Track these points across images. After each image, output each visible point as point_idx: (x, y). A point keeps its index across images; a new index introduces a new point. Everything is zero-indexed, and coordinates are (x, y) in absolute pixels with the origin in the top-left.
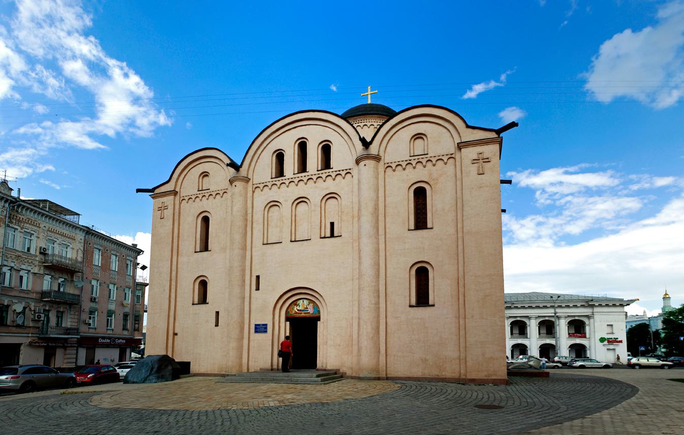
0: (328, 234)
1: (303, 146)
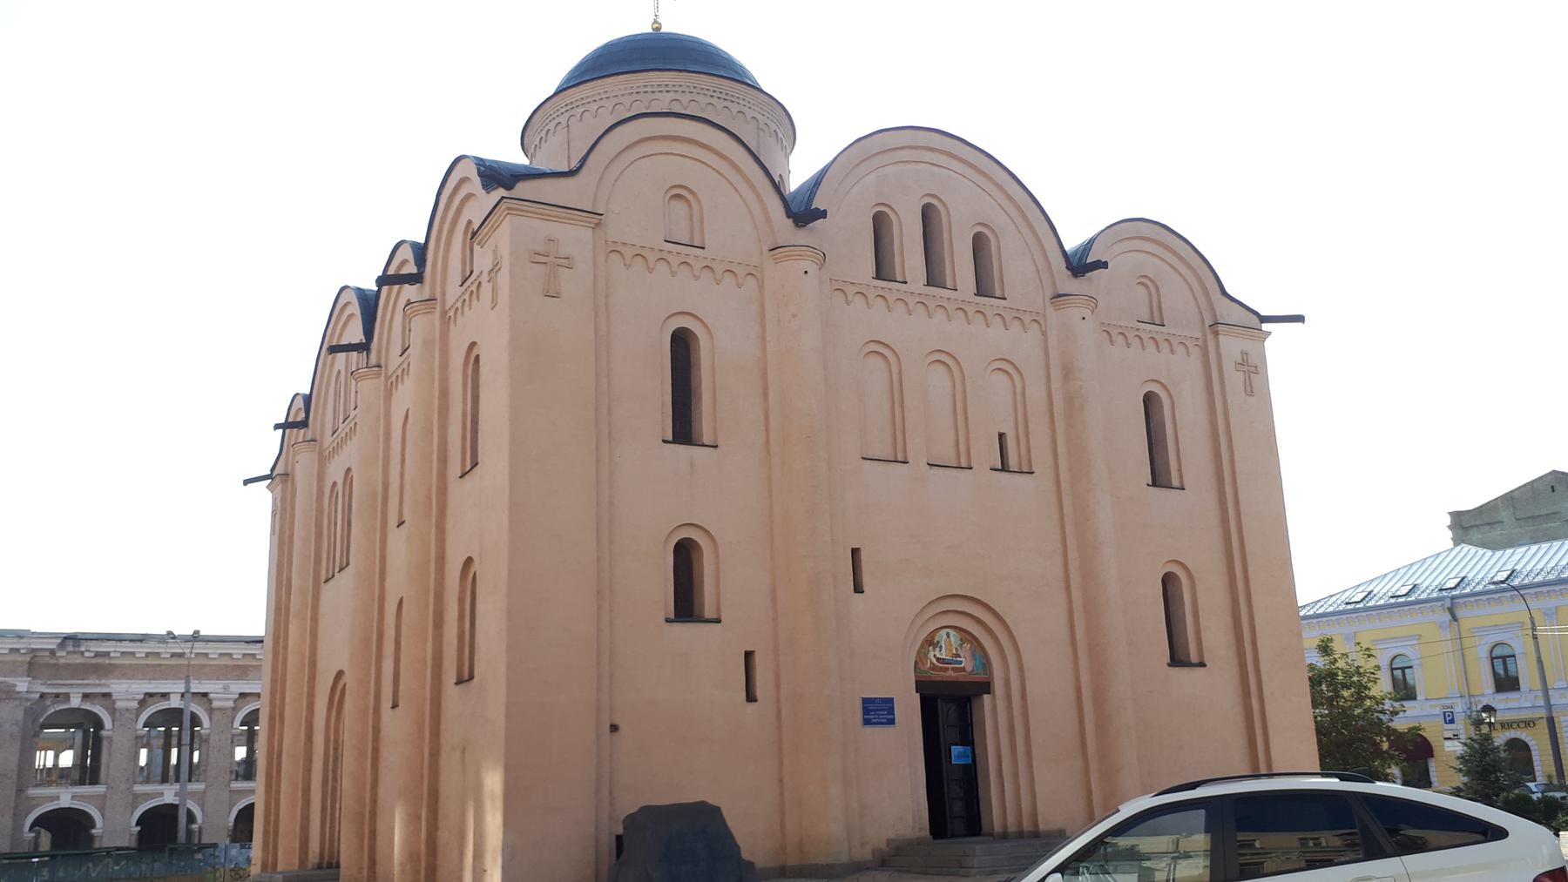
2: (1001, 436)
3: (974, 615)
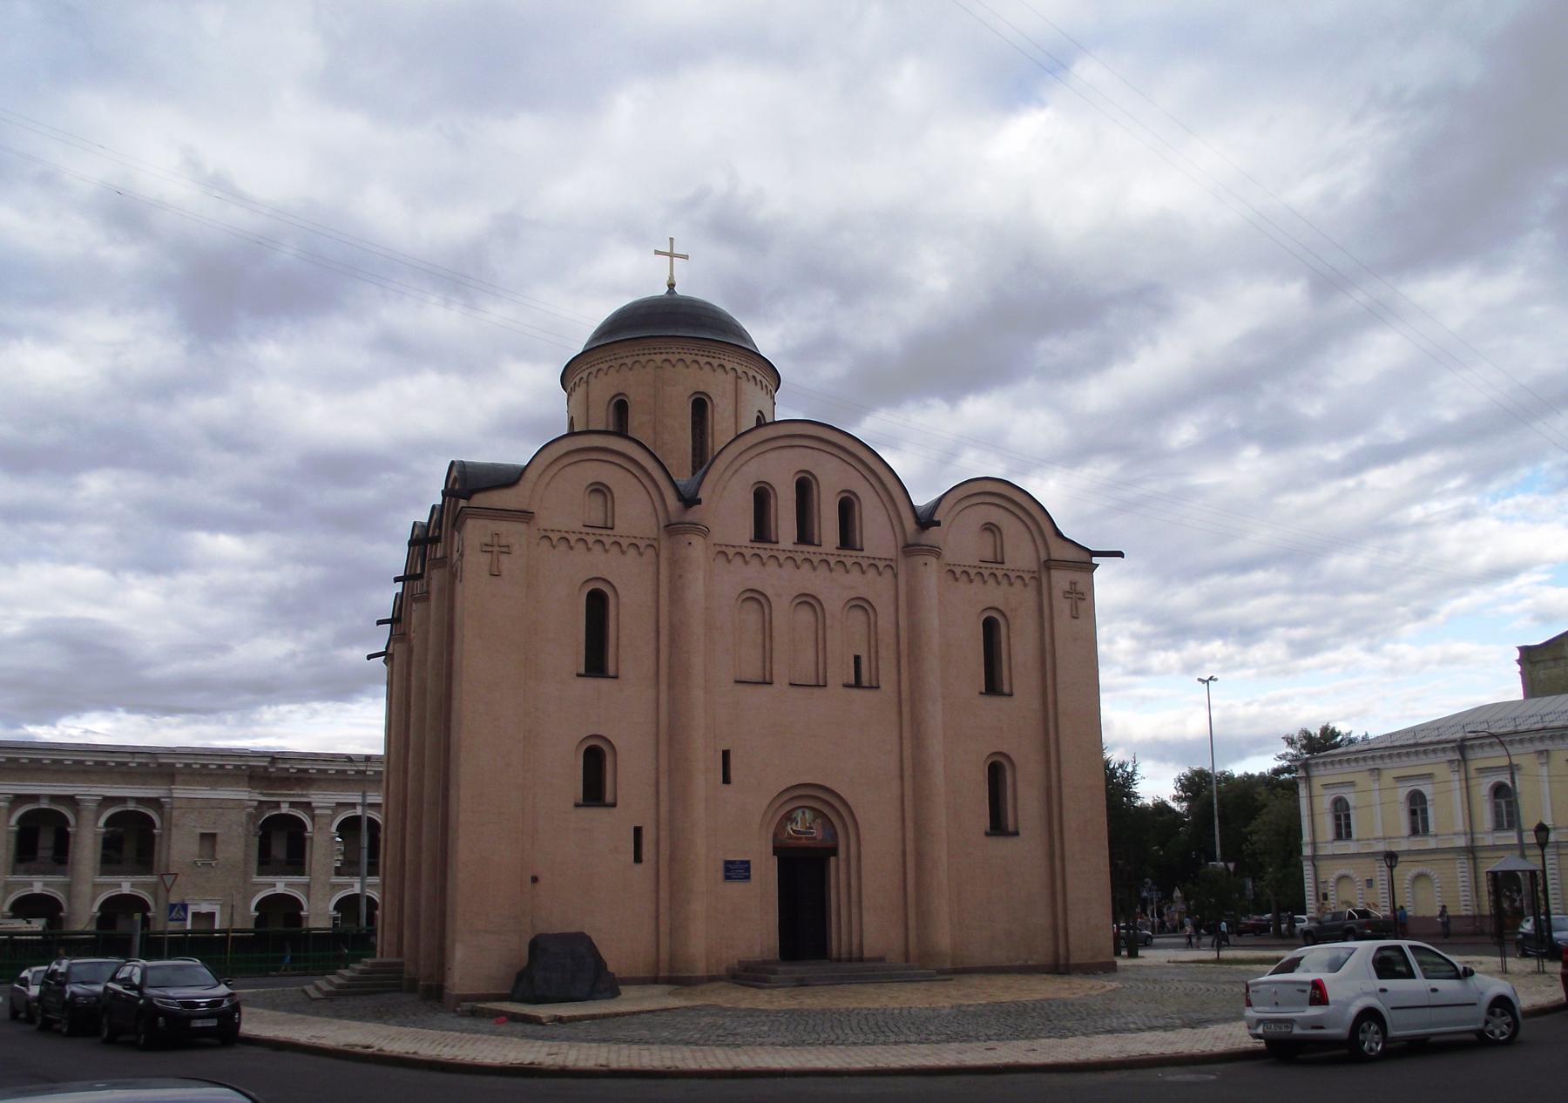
0: (852, 680)
1: (804, 488)
2: (857, 659)
3: (820, 800)
